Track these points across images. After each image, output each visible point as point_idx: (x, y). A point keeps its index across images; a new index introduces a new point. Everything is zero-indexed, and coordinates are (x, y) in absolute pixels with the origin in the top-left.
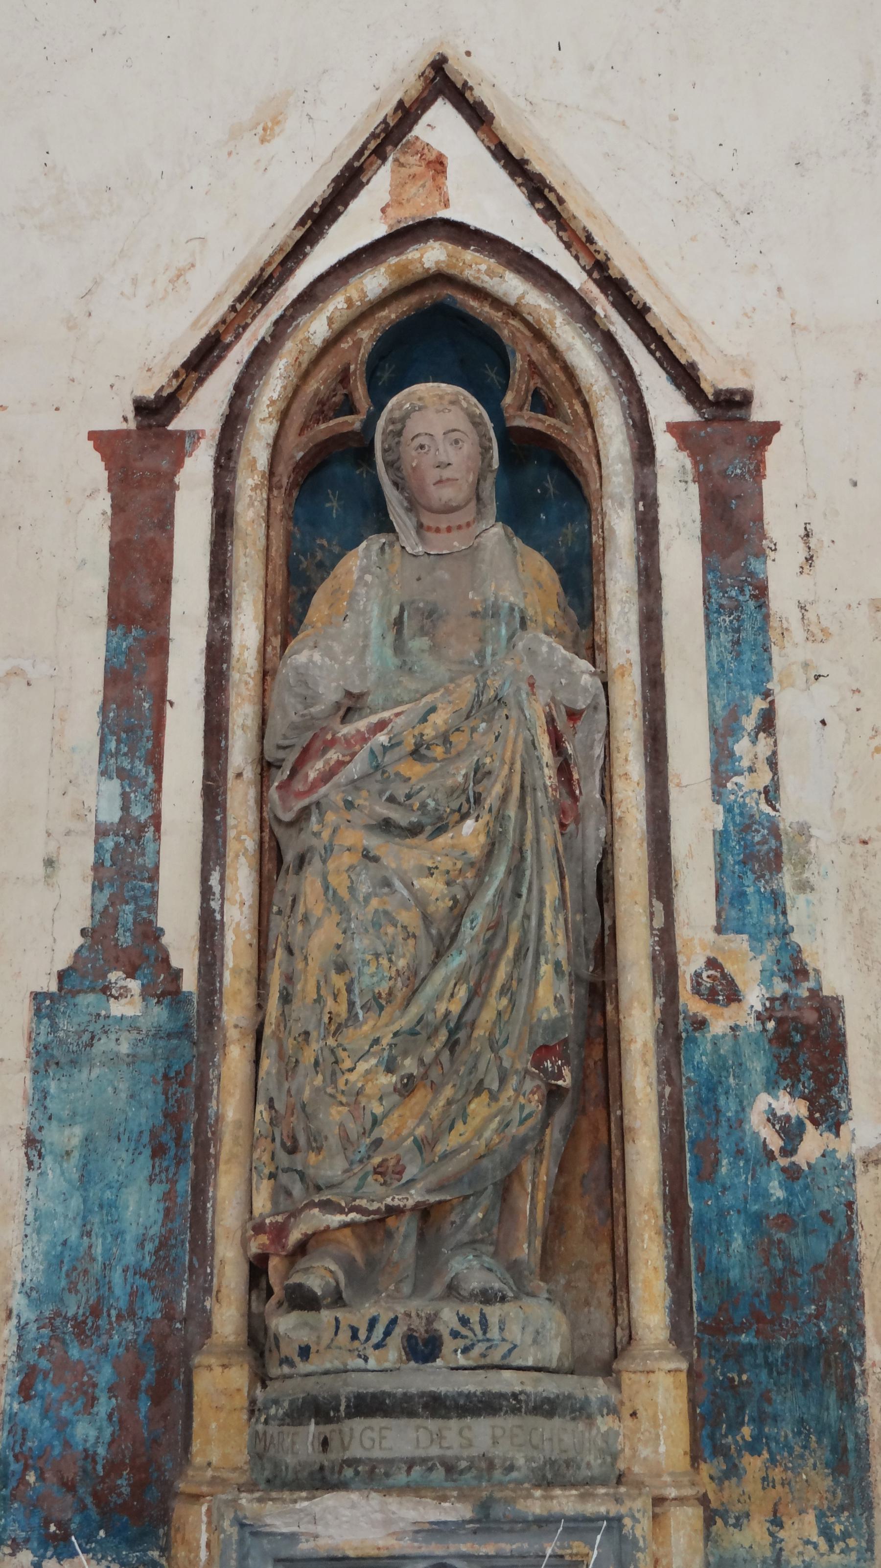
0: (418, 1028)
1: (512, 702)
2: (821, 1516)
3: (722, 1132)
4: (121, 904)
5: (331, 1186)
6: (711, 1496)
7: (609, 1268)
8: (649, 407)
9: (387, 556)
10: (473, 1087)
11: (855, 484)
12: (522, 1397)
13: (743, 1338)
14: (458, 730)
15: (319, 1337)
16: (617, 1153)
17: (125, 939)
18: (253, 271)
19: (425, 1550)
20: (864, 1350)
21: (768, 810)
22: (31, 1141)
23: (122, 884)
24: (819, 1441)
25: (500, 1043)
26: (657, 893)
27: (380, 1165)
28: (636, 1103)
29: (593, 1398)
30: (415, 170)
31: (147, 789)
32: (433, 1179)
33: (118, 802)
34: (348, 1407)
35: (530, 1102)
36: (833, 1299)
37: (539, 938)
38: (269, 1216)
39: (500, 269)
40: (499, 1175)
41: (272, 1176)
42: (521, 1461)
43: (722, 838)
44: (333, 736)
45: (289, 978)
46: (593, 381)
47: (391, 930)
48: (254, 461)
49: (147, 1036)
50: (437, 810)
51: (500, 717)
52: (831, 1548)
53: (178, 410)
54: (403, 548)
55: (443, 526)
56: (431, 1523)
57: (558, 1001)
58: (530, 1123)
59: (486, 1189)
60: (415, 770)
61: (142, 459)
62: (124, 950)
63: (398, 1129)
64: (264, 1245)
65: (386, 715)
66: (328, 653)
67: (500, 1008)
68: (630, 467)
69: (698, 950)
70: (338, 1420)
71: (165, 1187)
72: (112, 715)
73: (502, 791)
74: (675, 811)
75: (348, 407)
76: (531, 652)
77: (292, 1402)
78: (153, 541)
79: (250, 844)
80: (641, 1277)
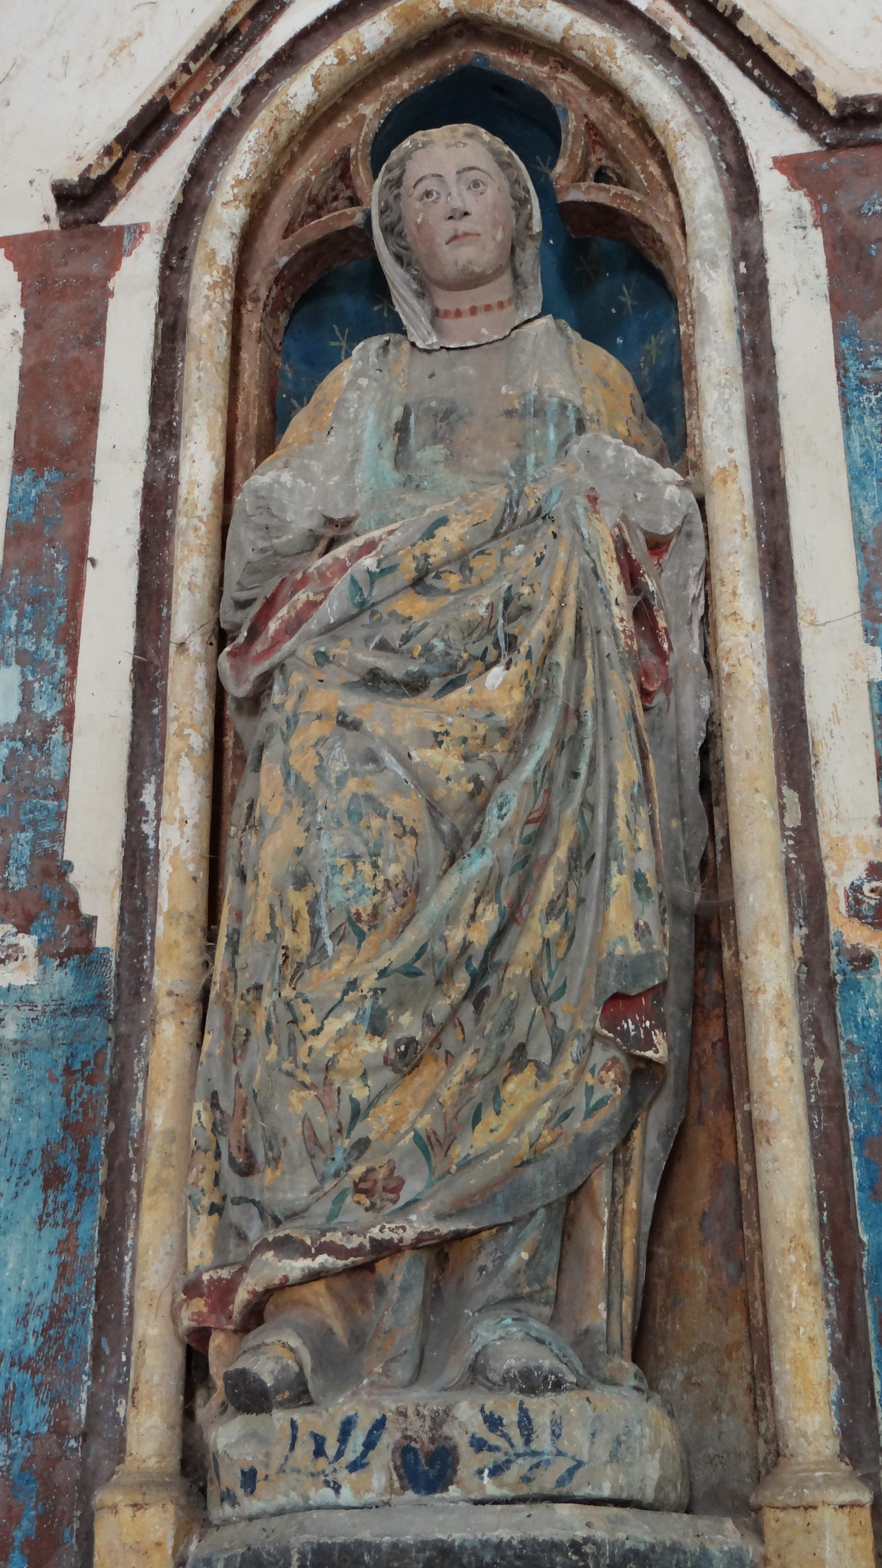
0: (418, 965)
1: (563, 518)
4: (14, 832)
5: (293, 1215)
8: (748, 141)
9: (390, 357)
10: (508, 1053)
12: (588, 1549)
14: (482, 553)
15: (267, 1455)
16: (747, 1168)
17: (18, 879)
23: (18, 805)
25: (551, 991)
26: (789, 778)
27: (363, 1179)
28: (770, 1083)
29: (714, 1550)
31: (57, 676)
32: (445, 1197)
35: (602, 1082)
37: (609, 838)
38: (207, 1271)
40: (555, 1192)
41: (215, 1209)
44: (304, 573)
46: (669, 117)
47: (376, 822)
48: (214, 253)
49: (44, 1012)
50: (447, 654)
51: (544, 534)
54: (413, 344)
55: (465, 307)
57: (641, 931)
58: (603, 1114)
59: (533, 1214)
61: (66, 264)
62: (16, 894)
63: (393, 1124)
64: (199, 1314)
65: (376, 534)
66: (304, 472)
67: (548, 934)
69: (855, 853)
71: (61, 1232)
72: (13, 582)
73: (547, 632)
74: (807, 660)
76: (592, 459)
78: (77, 361)
80: (789, 1354)
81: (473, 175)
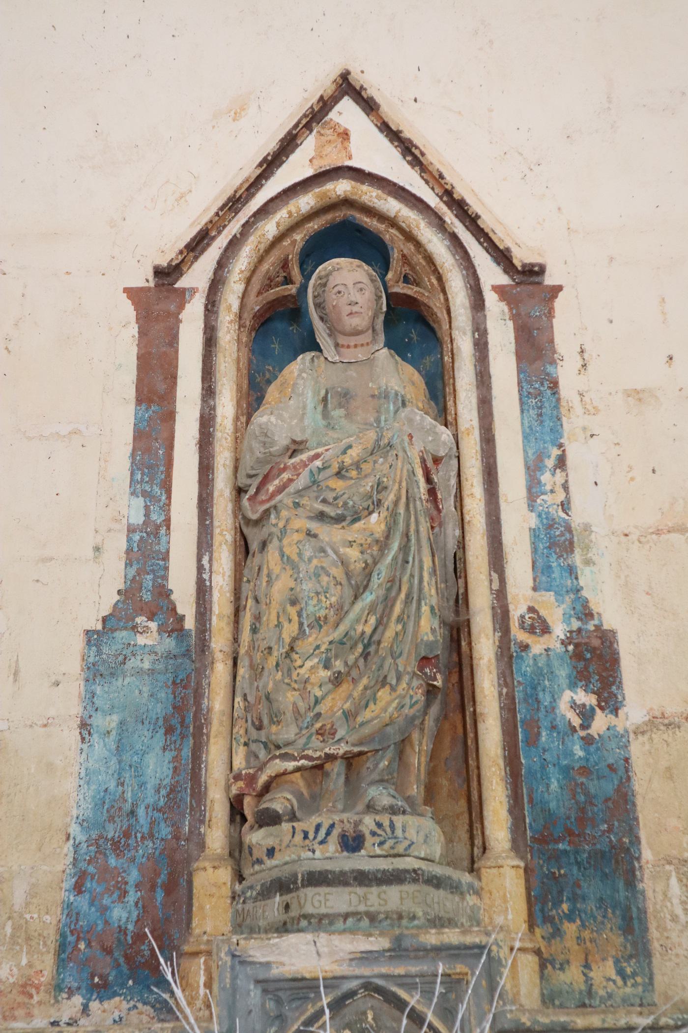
0: (345, 640)
2: (617, 962)
3: (542, 714)
4: (144, 575)
5: (288, 744)
6: (543, 949)
7: (466, 815)
8: (480, 276)
9: (316, 364)
10: (381, 679)
11: (611, 322)
12: (420, 872)
13: (561, 846)
14: (365, 461)
15: (281, 841)
17: (147, 597)
18: (229, 193)
19: (358, 972)
20: (641, 853)
21: (564, 515)
22: (84, 725)
23: (145, 563)
24: (614, 913)
25: (397, 654)
26: (494, 568)
27: (320, 729)
28: (485, 697)
29: (463, 882)
30: (330, 138)
31: (162, 504)
33: (142, 512)
34: (303, 880)
35: (416, 694)
36: (618, 820)
37: (420, 589)
38: (244, 769)
39: (385, 196)
40: (398, 738)
41: (246, 744)
42: (420, 914)
43: (534, 534)
44: (285, 465)
45: (258, 618)
46: (444, 261)
48: (229, 308)
49: (162, 657)
50: (354, 507)
51: (392, 455)
52: (625, 983)
53: (182, 275)
54: (326, 359)
55: (352, 344)
56: (362, 952)
57: (433, 631)
58: (417, 707)
59: (389, 746)
60: (339, 485)
61: (158, 304)
62: (146, 603)
63: (331, 707)
64: (241, 788)
65: (319, 450)
66: (280, 417)
67: (397, 630)
68: (469, 311)
69: (522, 601)
70: (297, 889)
71: (174, 753)
72: (138, 458)
73: (395, 499)
74: (504, 517)
75: (288, 280)
76: (410, 421)
77: (262, 885)
78: (165, 353)
79: (229, 537)
80: (491, 808)
81: (360, 286)
